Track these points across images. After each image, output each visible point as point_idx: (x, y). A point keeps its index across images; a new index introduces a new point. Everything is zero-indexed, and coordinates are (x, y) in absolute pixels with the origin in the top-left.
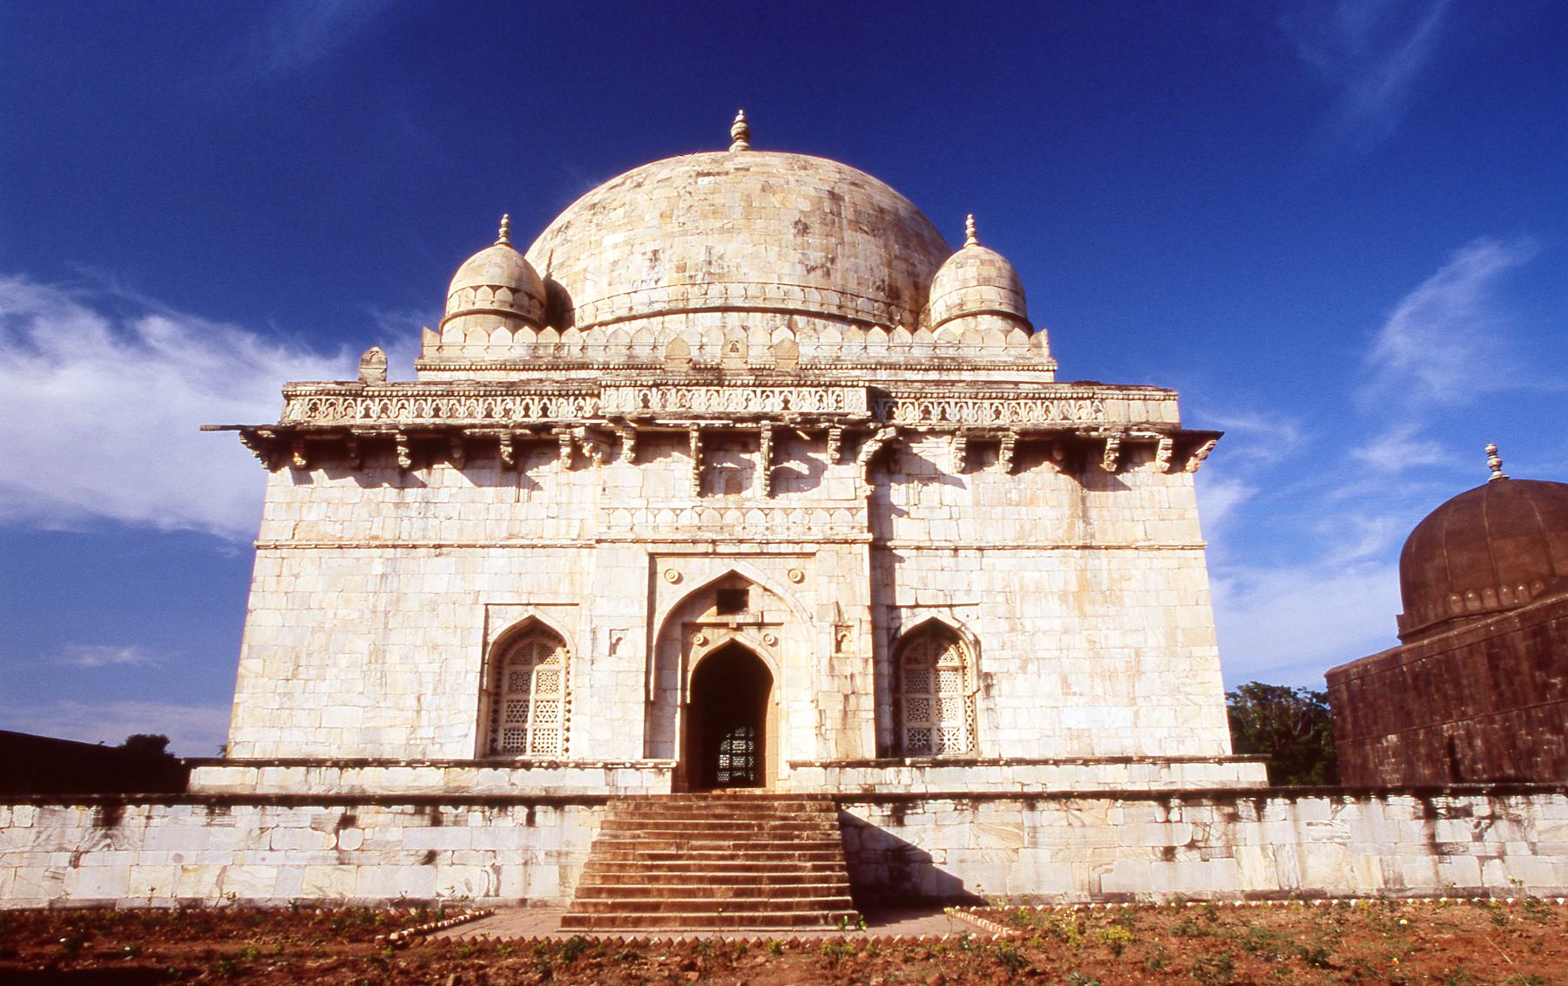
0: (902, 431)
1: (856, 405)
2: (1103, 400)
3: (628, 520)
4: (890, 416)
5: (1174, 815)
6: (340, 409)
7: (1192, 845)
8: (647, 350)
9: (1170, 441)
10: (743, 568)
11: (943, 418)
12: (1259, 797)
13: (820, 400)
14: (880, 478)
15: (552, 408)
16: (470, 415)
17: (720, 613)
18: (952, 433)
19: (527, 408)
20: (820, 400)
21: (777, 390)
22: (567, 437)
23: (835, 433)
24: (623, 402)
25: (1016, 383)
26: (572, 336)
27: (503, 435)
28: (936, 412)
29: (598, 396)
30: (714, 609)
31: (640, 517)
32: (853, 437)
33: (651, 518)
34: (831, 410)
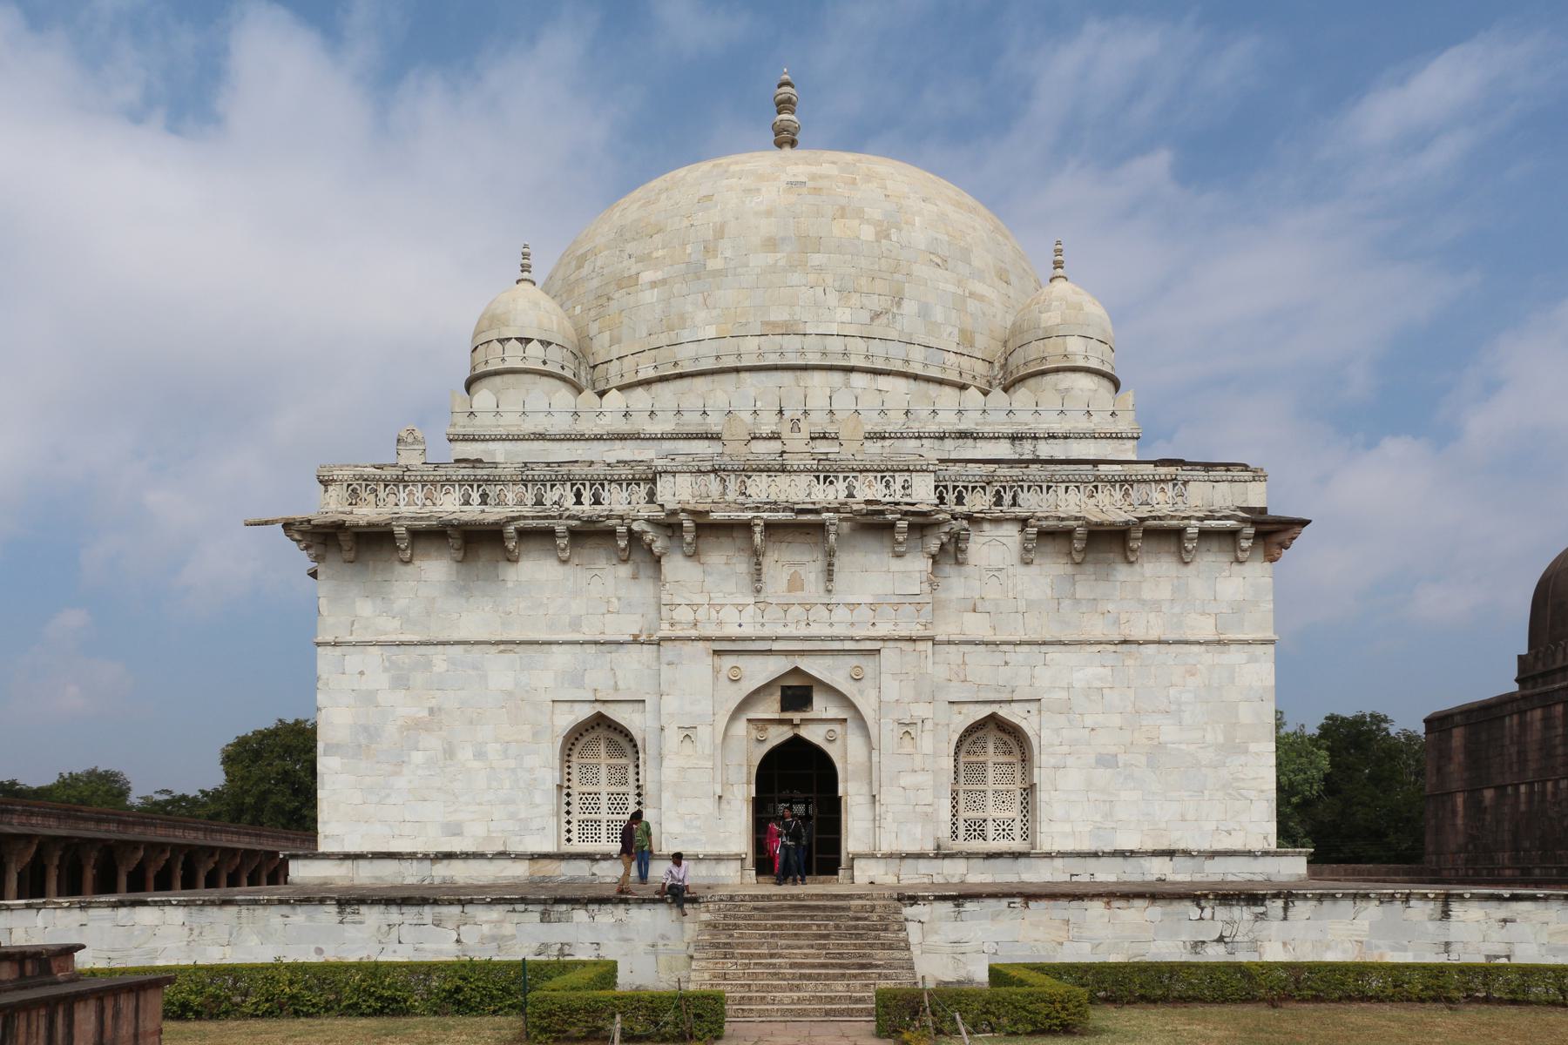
0: (969, 518)
1: (923, 493)
2: (1185, 483)
3: (691, 617)
4: (960, 500)
5: (1207, 913)
6: (382, 495)
7: (1221, 939)
8: (697, 417)
9: (1251, 531)
10: (806, 665)
11: (1014, 504)
12: (1288, 896)
13: (887, 486)
14: (948, 569)
15: (605, 494)
16: (521, 503)
17: (784, 709)
18: (1024, 522)
19: (578, 495)
20: (887, 486)
21: (841, 476)
22: (623, 529)
23: (903, 524)
24: (677, 492)
25: (1095, 463)
26: (614, 399)
27: (560, 528)
28: (1007, 498)
29: (654, 481)
30: (777, 706)
31: (702, 614)
32: (922, 525)
33: (713, 613)
34: (897, 498)
